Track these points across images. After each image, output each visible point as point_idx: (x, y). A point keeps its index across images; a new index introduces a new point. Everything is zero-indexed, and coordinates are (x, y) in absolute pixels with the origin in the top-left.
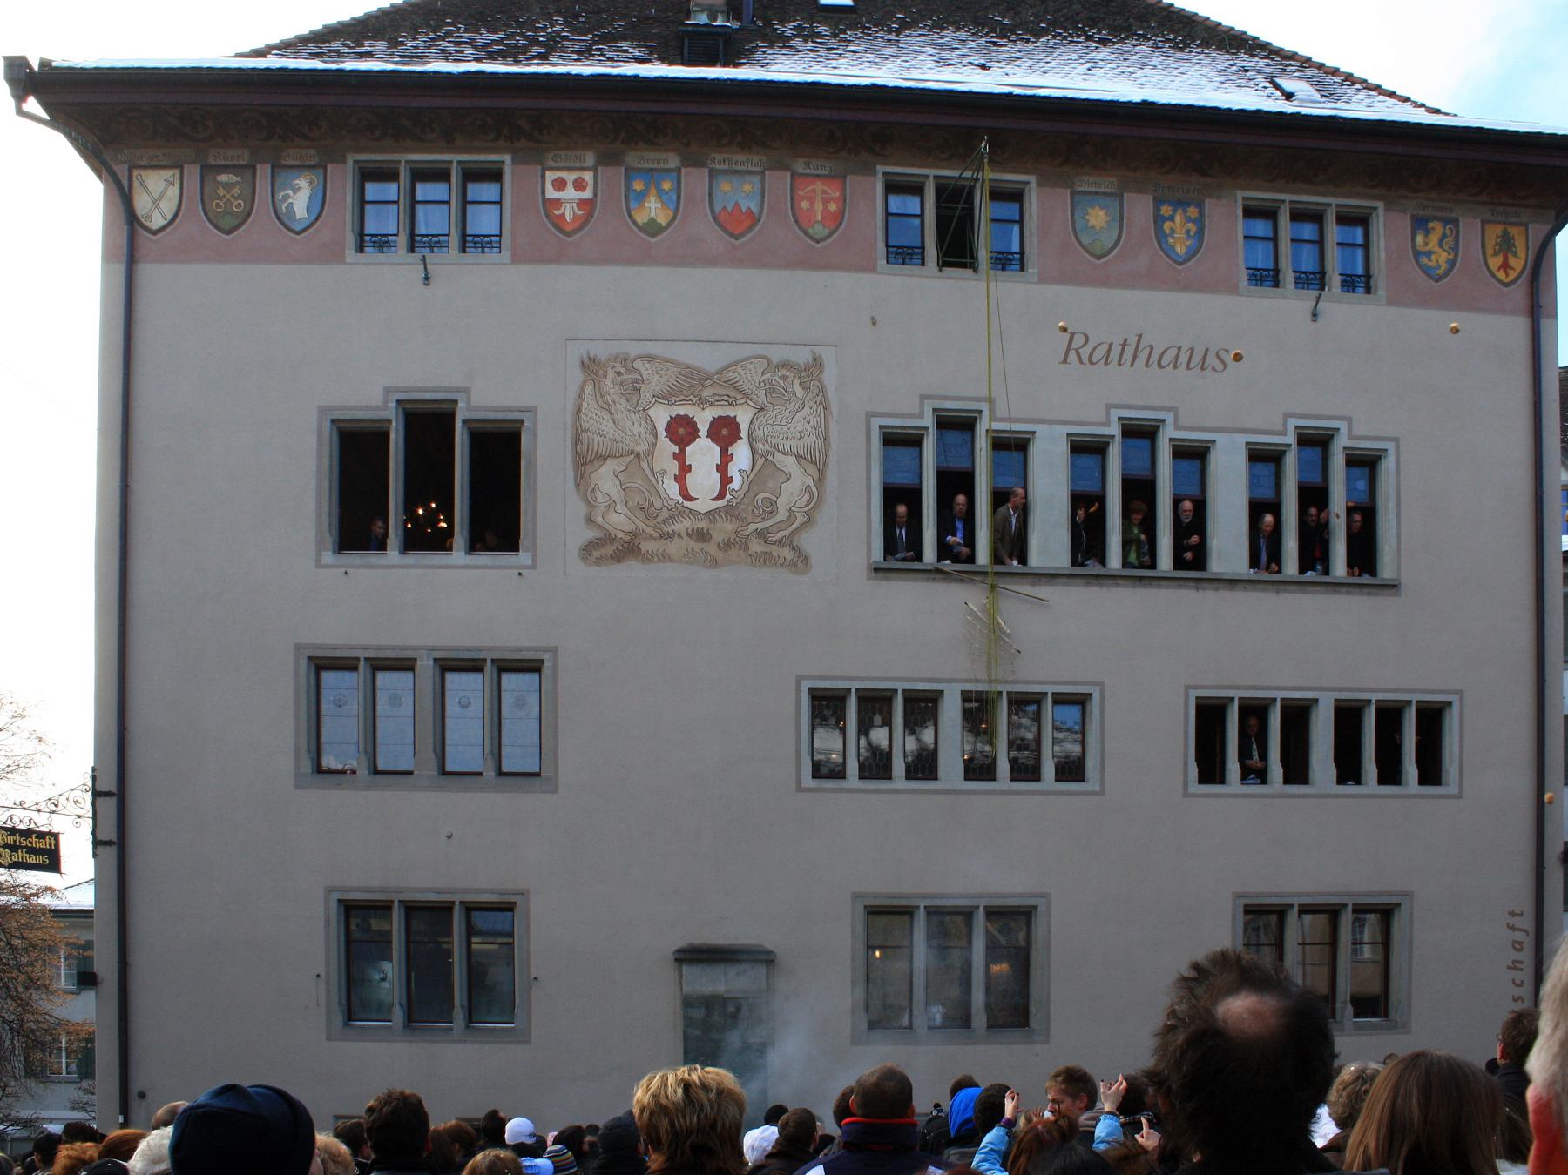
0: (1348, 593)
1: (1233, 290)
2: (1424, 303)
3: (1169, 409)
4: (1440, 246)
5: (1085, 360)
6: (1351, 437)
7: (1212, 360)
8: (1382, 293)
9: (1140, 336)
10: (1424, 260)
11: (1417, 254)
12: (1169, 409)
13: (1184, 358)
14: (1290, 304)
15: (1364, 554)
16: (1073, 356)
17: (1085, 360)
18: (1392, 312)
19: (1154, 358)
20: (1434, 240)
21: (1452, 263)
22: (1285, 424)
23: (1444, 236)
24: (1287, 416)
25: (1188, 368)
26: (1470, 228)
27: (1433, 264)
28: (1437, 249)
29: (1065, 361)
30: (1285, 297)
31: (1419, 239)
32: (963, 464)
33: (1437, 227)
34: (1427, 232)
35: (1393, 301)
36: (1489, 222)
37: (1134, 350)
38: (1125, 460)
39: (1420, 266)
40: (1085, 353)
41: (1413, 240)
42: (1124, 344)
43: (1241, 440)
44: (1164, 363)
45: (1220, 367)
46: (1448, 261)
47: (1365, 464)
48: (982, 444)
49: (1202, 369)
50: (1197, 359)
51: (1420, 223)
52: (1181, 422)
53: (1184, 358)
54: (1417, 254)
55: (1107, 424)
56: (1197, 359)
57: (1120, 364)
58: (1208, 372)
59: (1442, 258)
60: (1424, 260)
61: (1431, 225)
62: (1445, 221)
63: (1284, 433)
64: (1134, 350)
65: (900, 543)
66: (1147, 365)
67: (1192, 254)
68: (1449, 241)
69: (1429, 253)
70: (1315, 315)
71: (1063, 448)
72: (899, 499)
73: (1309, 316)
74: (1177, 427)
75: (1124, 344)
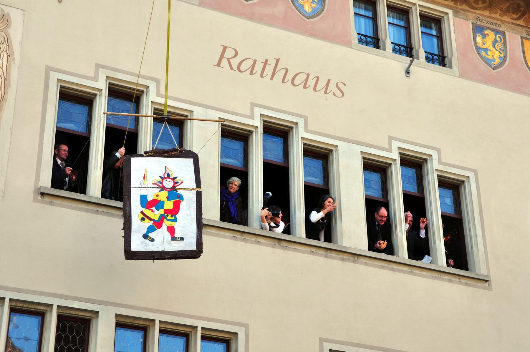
0: (450, 281)
1: (348, 44)
2: (487, 80)
3: (301, 116)
4: (494, 47)
5: (235, 67)
6: (440, 162)
7: (332, 87)
8: (455, 68)
9: (278, 60)
10: (483, 53)
11: (478, 49)
12: (301, 116)
13: (311, 82)
14: (387, 63)
15: (458, 255)
16: (224, 62)
17: (235, 67)
18: (465, 83)
19: (289, 77)
20: (489, 43)
21: (504, 60)
22: (390, 144)
23: (495, 42)
24: (391, 139)
25: (315, 89)
26: (514, 38)
27: (490, 57)
28: (492, 48)
29: (219, 65)
30: (385, 57)
31: (479, 39)
32: (129, 126)
33: (491, 36)
34: (484, 36)
35: (462, 75)
36: (526, 38)
37: (271, 68)
38: (265, 149)
39: (481, 57)
40: (235, 62)
41: (475, 38)
42: (266, 63)
43: (359, 149)
44: (296, 82)
45: (339, 94)
46: (500, 57)
47: (452, 186)
48: (147, 109)
49: (326, 93)
50: (322, 84)
51: (478, 29)
52: (310, 128)
53: (311, 82)
54: (478, 49)
55: (252, 117)
56: (322, 84)
57: (262, 76)
58: (330, 96)
59: (495, 55)
60: (483, 53)
61: (486, 32)
62: (497, 32)
63: (390, 150)
64: (271, 68)
65: (68, 175)
66: (283, 82)
67: (315, 14)
68: (499, 45)
69: (486, 50)
70: (408, 72)
71: (216, 128)
72: (72, 147)
73: (404, 73)
74: (307, 130)
75: (266, 63)
